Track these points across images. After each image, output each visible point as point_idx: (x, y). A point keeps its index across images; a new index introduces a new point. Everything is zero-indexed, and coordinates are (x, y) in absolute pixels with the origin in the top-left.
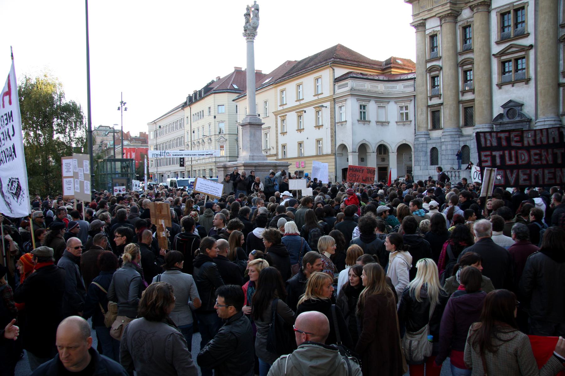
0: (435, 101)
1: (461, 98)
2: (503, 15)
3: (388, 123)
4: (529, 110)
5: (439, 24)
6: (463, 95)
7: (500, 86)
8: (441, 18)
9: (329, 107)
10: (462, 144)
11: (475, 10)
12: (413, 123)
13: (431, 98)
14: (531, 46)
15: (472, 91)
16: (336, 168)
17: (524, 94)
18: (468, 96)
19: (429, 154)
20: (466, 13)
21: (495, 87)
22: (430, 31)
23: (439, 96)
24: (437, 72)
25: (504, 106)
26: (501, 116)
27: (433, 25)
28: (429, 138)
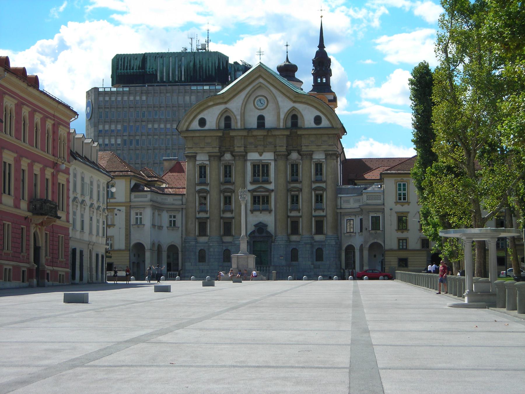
0: (203, 215)
1: (222, 215)
2: (256, 167)
3: (162, 227)
4: (271, 228)
5: (208, 159)
6: (223, 213)
7: (252, 211)
8: (210, 156)
9: (124, 211)
10: (224, 248)
11: (237, 158)
12: (180, 229)
13: (199, 212)
14: (273, 190)
15: (231, 211)
16: (130, 261)
17: (268, 219)
18: (228, 215)
19: (197, 254)
20: (228, 156)
21: (249, 212)
22: (200, 162)
23: (206, 212)
24: (205, 194)
25: (256, 226)
26: (253, 232)
27: (202, 158)
28: (197, 242)
